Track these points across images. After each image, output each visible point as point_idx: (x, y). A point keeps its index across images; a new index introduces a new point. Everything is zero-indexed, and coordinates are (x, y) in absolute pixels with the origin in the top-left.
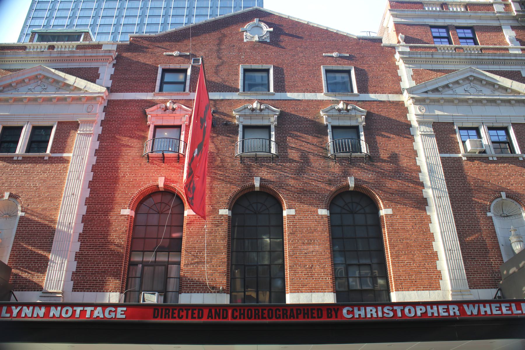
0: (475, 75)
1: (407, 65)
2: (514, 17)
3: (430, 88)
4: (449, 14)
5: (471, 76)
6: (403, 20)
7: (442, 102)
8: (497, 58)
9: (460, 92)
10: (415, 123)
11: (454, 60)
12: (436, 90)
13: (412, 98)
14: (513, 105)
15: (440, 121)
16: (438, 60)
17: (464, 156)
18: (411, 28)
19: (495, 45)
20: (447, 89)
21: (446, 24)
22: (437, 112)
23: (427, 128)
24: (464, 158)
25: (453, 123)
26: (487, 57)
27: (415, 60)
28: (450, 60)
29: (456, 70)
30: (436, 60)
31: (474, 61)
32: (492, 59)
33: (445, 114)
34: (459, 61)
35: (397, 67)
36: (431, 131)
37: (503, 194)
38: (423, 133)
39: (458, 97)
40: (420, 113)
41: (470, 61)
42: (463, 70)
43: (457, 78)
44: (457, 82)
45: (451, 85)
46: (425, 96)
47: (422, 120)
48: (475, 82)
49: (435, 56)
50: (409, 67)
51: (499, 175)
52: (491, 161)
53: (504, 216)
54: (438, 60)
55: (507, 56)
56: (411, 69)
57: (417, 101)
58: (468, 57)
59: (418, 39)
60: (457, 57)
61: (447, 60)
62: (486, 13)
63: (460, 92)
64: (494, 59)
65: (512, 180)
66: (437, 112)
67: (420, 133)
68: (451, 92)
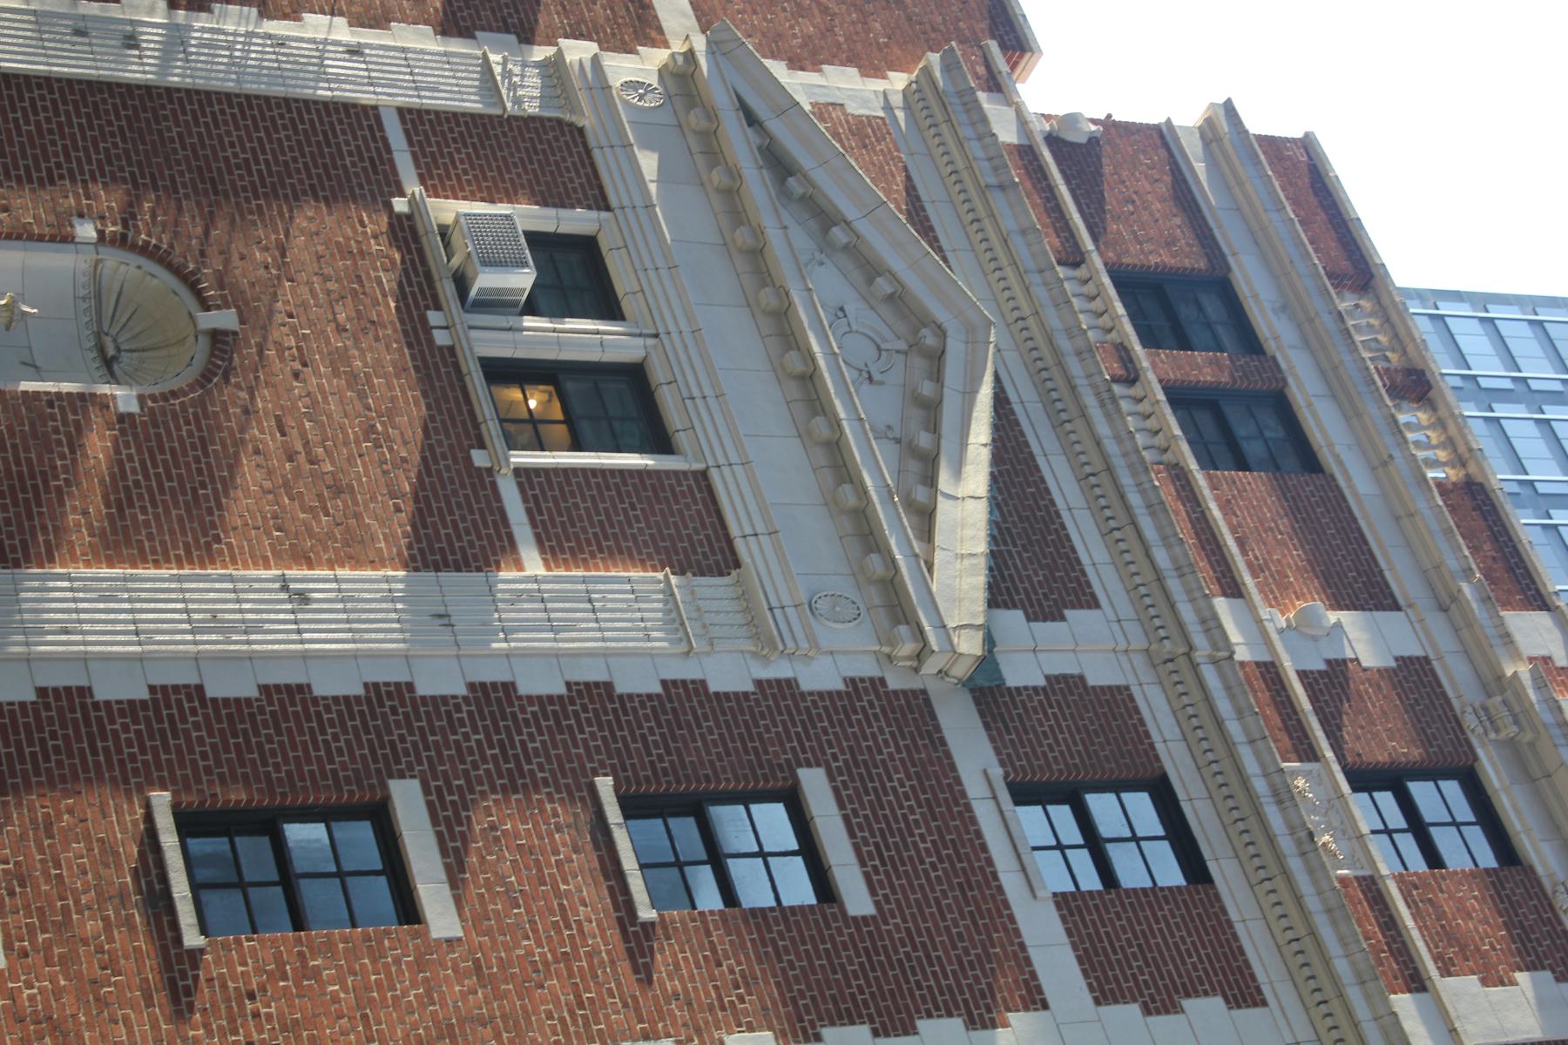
0: (955, 349)
1: (896, 100)
2: (1500, 677)
3: (774, 125)
4: (1347, 358)
5: (941, 333)
6: (1200, 167)
7: (717, 177)
8: (1126, 480)
9: (819, 293)
10: (540, 53)
11: (1018, 291)
12: (778, 164)
13: (690, 55)
14: (831, 504)
15: (596, 153)
16: (987, 223)
17: (412, 202)
18: (1163, 188)
19: (1241, 543)
20: (813, 225)
21: (1271, 346)
22: (648, 163)
23: (536, 93)
24: (400, 205)
25: (608, 208)
26: (1103, 429)
27: (944, 128)
28: (1009, 272)
29: (934, 242)
30: (981, 212)
31: (1060, 382)
32: (1105, 457)
33: (653, 188)
34: (1026, 310)
35: (872, 69)
36: (518, 101)
37: (225, 319)
38: (497, 69)
39: (797, 298)
40: (616, 82)
41: (1049, 360)
42: (960, 286)
43: (896, 263)
44: (869, 268)
45: (838, 234)
46: (721, 100)
47: (577, 83)
48: (919, 363)
49: (998, 201)
50: (888, 107)
51: (341, 329)
52: (424, 320)
53: (101, 349)
54: (987, 223)
55: (1159, 528)
56: (882, 114)
57: (681, 78)
58: (1064, 344)
59: (1101, 201)
60: (1040, 293)
61: (1004, 261)
62: (1448, 532)
63: (819, 293)
64: (1109, 469)
65: (320, 377)
66: (648, 163)
67: (495, 58)
68: (802, 240)
